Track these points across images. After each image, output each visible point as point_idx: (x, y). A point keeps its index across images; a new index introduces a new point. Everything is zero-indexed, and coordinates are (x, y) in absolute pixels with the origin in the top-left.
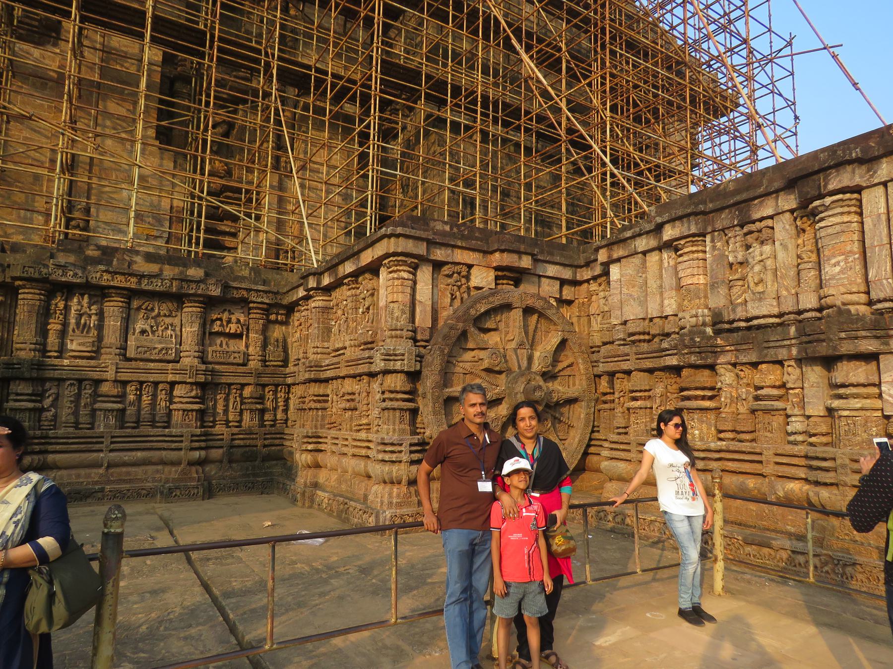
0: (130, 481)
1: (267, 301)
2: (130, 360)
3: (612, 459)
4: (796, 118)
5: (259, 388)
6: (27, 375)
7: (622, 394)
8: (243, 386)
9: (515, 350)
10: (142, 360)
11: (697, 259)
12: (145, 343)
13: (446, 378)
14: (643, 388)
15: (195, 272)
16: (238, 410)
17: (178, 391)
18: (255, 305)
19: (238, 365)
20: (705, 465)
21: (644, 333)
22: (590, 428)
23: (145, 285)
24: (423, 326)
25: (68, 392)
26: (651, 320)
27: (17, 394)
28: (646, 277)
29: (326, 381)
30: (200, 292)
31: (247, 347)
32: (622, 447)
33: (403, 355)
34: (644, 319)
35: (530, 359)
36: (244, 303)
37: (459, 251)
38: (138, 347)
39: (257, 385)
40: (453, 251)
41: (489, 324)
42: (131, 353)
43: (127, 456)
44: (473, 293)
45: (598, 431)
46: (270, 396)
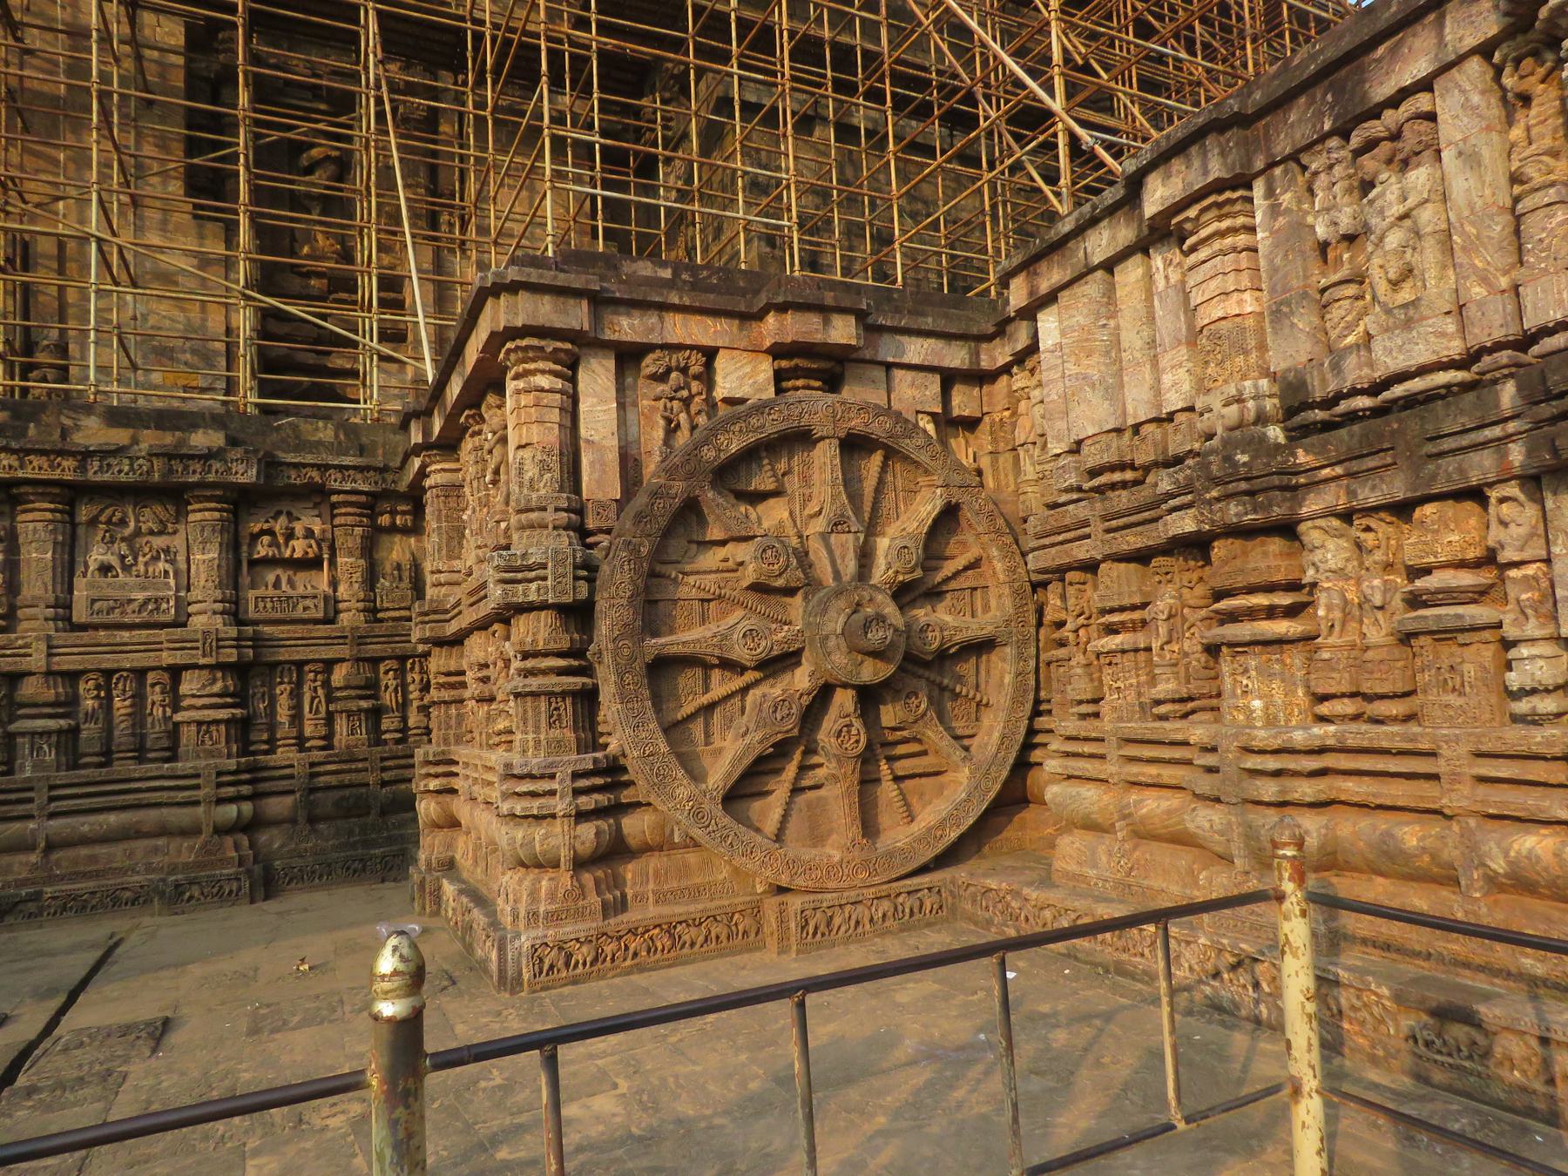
0: (97, 875)
1: (366, 488)
2: (83, 627)
3: (1070, 777)
5: (366, 672)
7: (1081, 620)
8: (329, 665)
9: (824, 536)
10: (106, 627)
11: (1234, 249)
12: (109, 592)
14: (1126, 602)
16: (323, 714)
18: (341, 498)
19: (316, 622)
20: (1282, 792)
21: (1122, 467)
22: (1029, 706)
24: (600, 496)
26: (1136, 428)
28: (1118, 327)
31: (334, 584)
32: (1087, 748)
33: (544, 567)
34: (1118, 431)
35: (865, 556)
36: (317, 495)
37: (679, 318)
38: (93, 601)
39: (358, 660)
40: (661, 318)
41: (762, 481)
42: (80, 614)
43: (86, 825)
44: (723, 410)
45: (1049, 712)
46: (389, 680)
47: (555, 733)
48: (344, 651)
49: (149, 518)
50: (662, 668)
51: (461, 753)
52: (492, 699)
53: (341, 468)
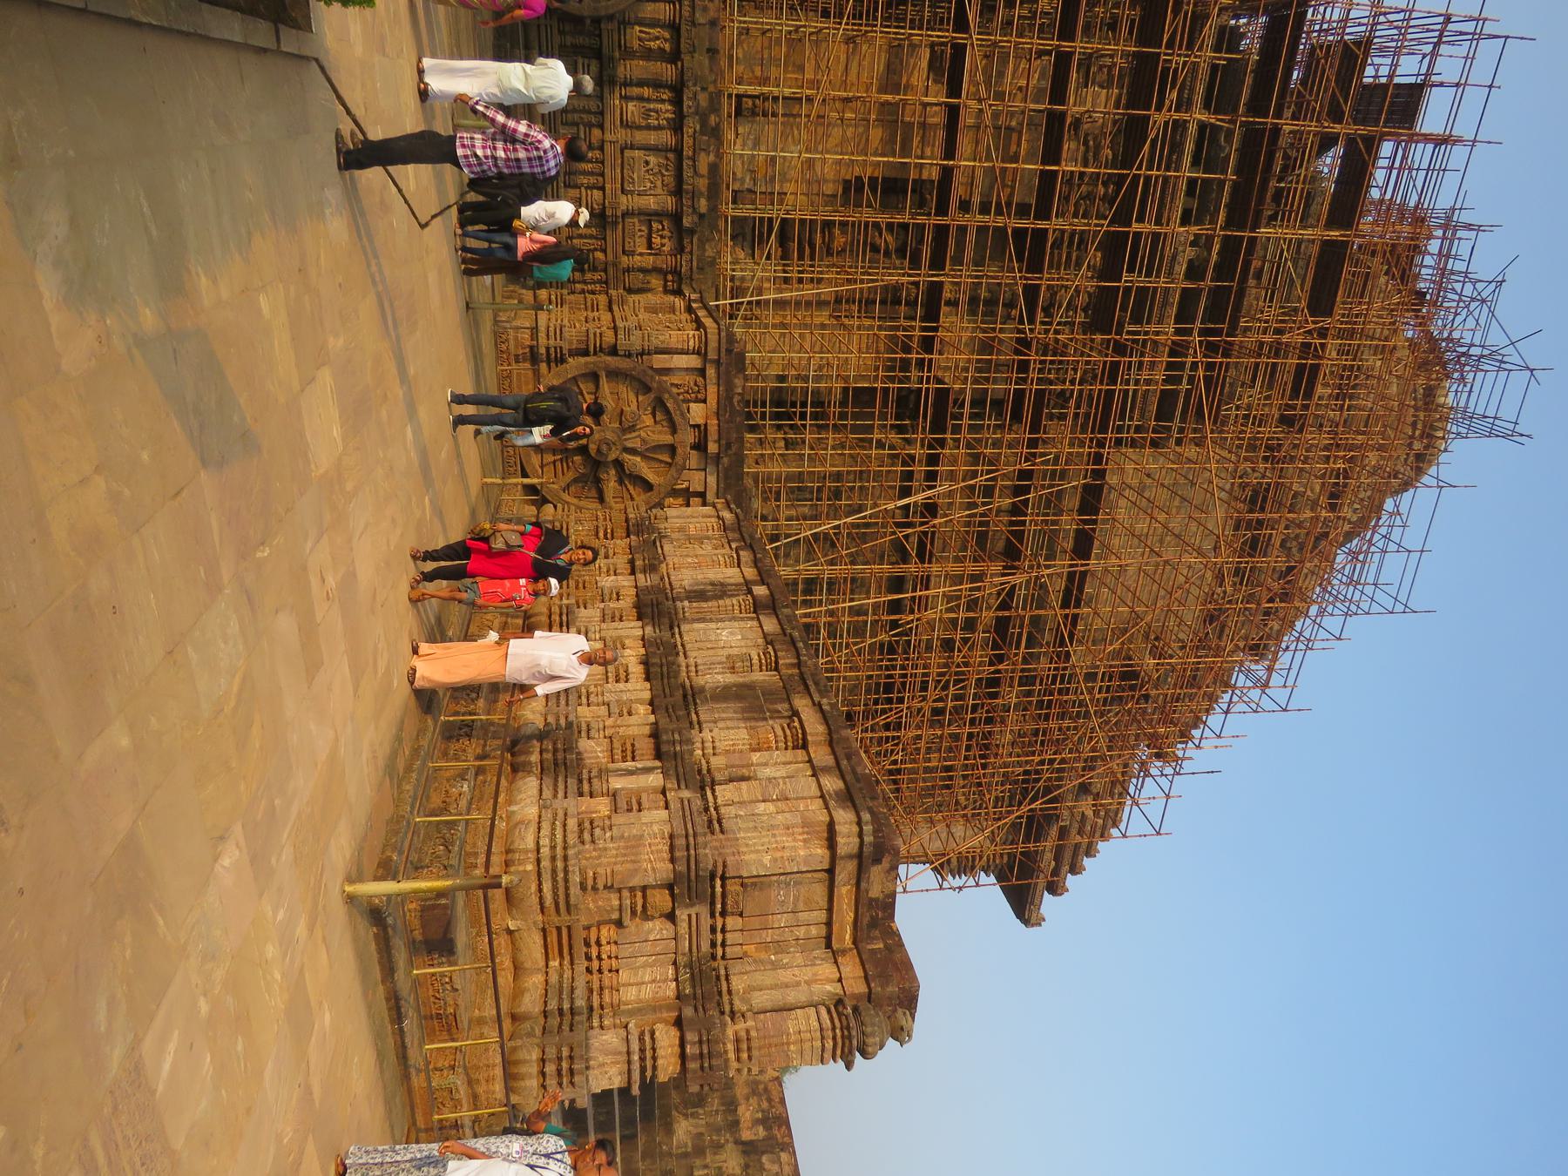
1: (683, 270)
2: (622, 153)
5: (603, 266)
9: (639, 436)
13: (614, 374)
15: (703, 205)
17: (597, 194)
19: (623, 247)
23: (686, 163)
27: (588, 66)
29: (611, 310)
30: (685, 208)
35: (632, 451)
36: (680, 249)
37: (716, 390)
39: (606, 264)
41: (659, 416)
42: (628, 153)
46: (597, 276)
47: (575, 342)
48: (610, 257)
49: (670, 179)
50: (594, 377)
51: (566, 308)
52: (586, 322)
53: (692, 260)
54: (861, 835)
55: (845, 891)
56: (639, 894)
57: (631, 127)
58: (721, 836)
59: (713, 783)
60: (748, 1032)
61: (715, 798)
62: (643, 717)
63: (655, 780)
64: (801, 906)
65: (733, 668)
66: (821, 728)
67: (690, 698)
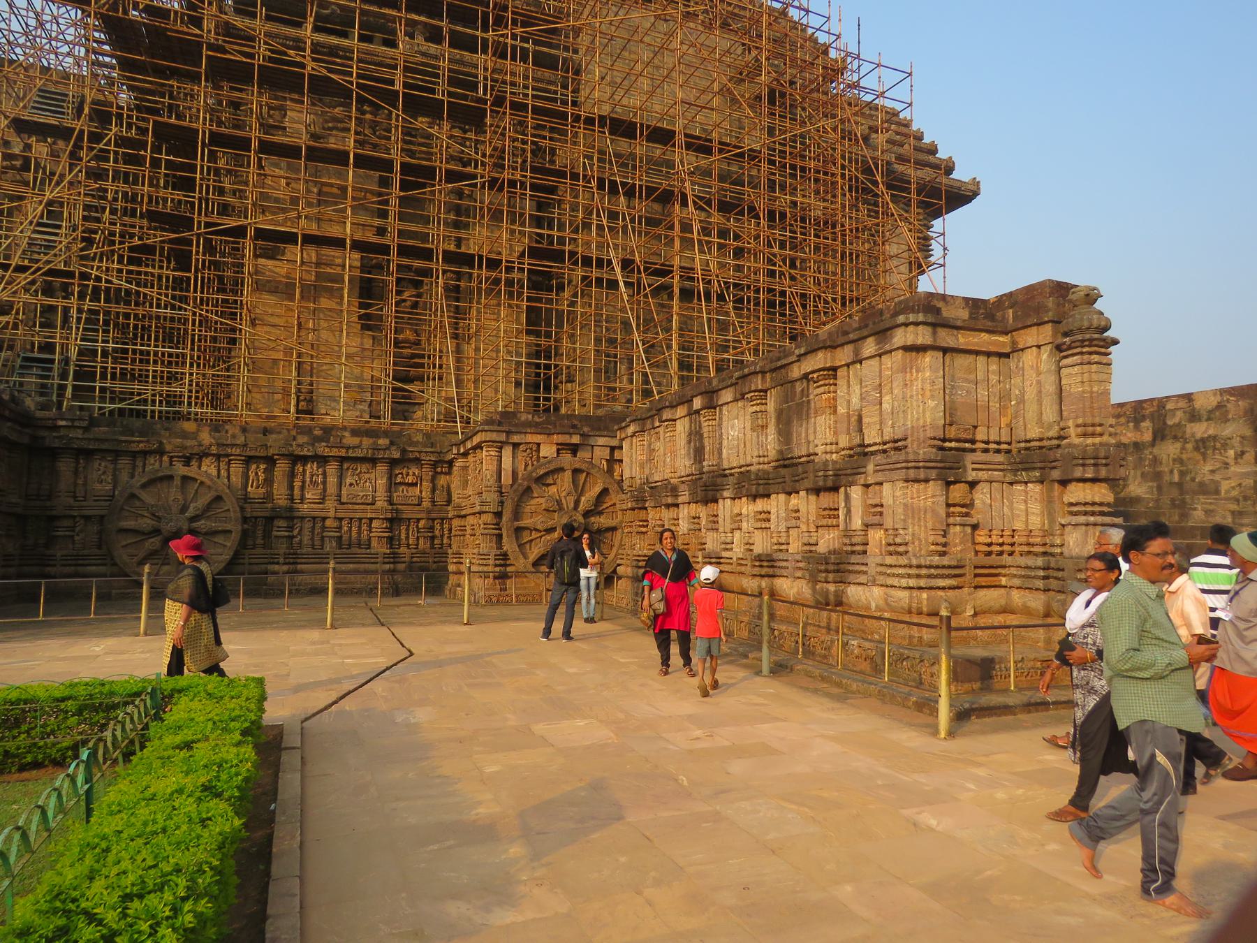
0: (347, 583)
2: (343, 504)
4: (945, 249)
5: (430, 523)
6: (284, 515)
8: (419, 520)
13: (517, 515)
15: (383, 442)
17: (375, 524)
23: (351, 454)
25: (308, 525)
29: (465, 516)
31: (421, 492)
35: (577, 503)
41: (550, 481)
42: (344, 499)
46: (438, 527)
49: (364, 467)
50: (519, 530)
51: (464, 551)
53: (426, 452)
54: (916, 324)
55: (963, 340)
56: (952, 509)
57: (325, 496)
58: (909, 440)
59: (863, 445)
60: (1078, 426)
61: (875, 444)
62: (804, 503)
63: (856, 493)
64: (972, 377)
65: (762, 426)
66: (820, 355)
67: (786, 462)
